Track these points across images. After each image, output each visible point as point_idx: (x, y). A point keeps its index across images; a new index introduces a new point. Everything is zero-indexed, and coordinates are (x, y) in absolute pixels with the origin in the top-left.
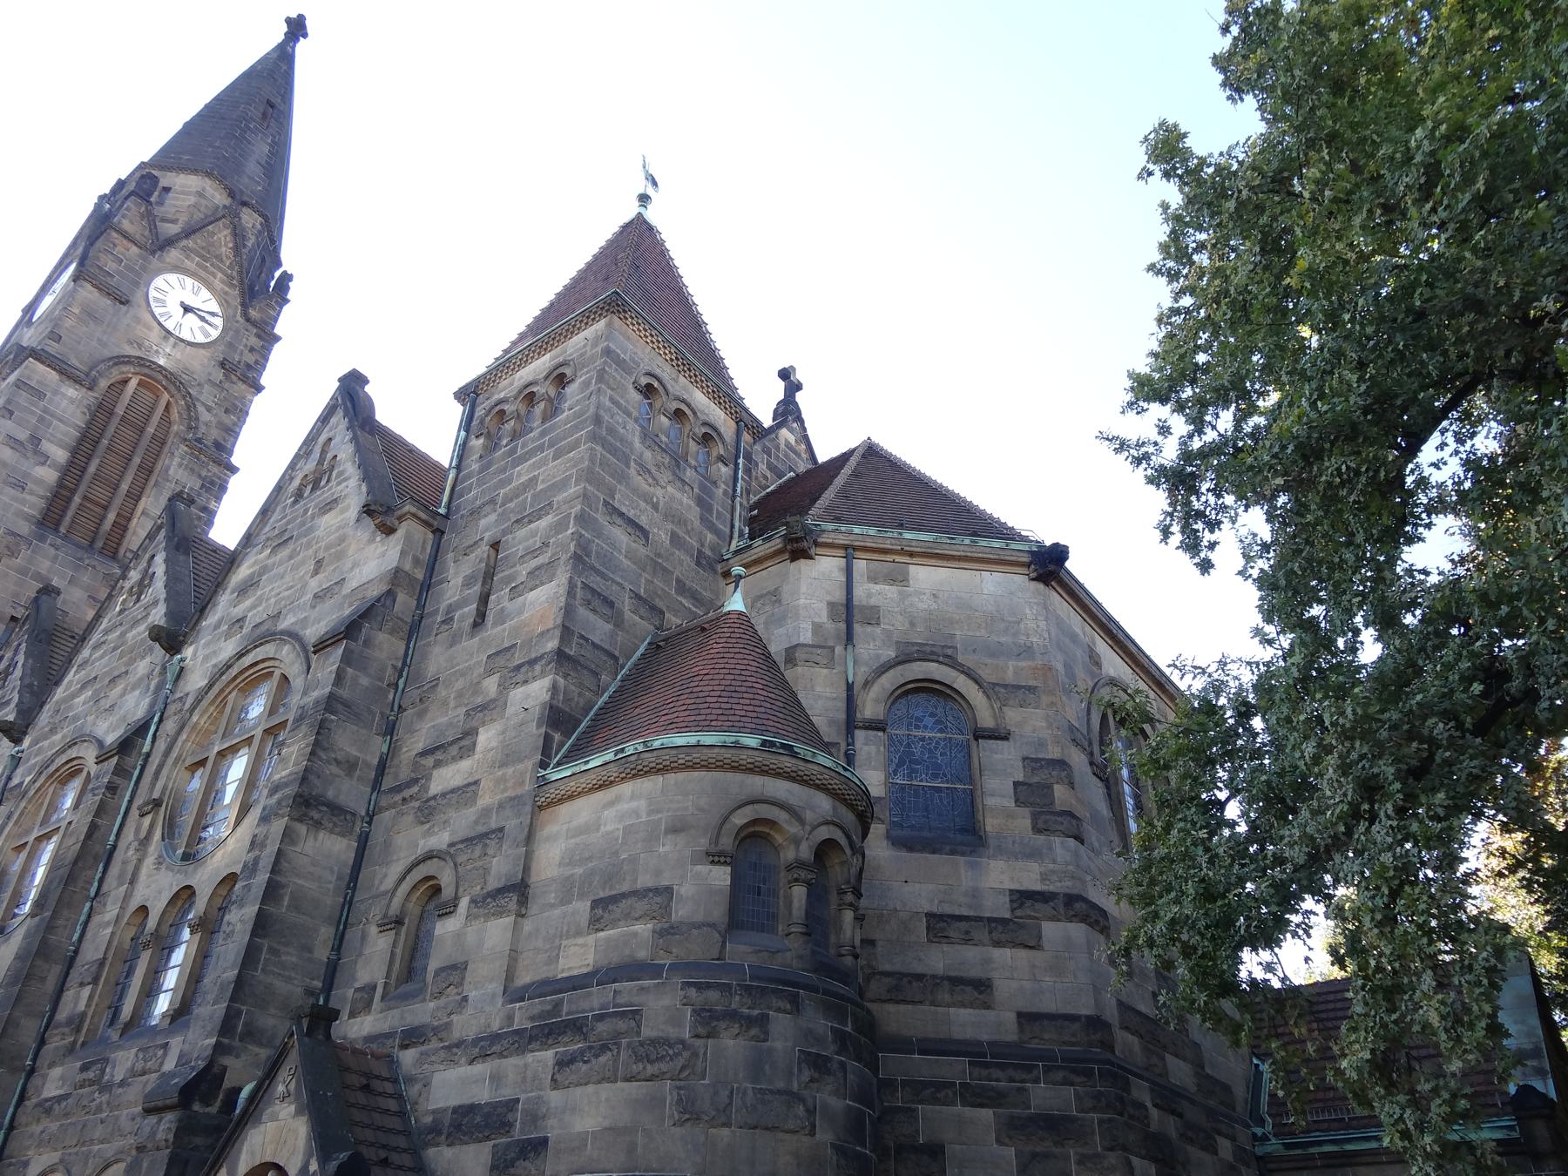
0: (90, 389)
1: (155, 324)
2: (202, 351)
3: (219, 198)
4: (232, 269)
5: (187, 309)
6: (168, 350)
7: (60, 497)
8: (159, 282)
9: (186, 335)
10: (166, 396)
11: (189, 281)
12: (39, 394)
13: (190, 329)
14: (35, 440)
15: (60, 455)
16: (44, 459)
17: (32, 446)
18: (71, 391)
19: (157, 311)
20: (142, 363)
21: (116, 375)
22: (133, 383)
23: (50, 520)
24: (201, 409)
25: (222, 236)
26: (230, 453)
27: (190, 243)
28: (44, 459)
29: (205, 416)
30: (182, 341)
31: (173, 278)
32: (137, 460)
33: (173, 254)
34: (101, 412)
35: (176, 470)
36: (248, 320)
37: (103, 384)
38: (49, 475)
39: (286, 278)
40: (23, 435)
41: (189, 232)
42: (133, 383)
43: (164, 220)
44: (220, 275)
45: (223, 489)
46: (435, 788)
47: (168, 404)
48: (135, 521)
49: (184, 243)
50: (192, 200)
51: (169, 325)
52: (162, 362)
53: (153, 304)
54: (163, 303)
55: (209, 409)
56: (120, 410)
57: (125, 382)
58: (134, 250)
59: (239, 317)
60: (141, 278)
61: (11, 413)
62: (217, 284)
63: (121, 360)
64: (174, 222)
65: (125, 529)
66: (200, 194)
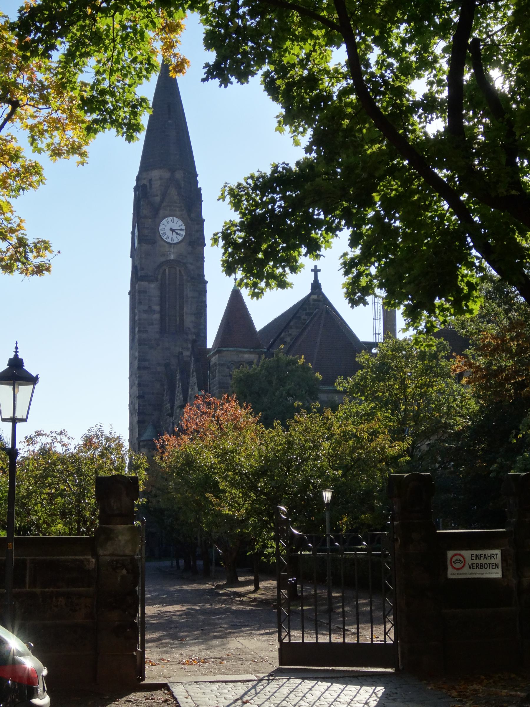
0: (157, 281)
1: (166, 244)
2: (183, 244)
3: (167, 175)
4: (179, 203)
5: (173, 230)
6: (172, 251)
7: (162, 319)
8: (161, 226)
9: (176, 241)
10: (178, 268)
11: (169, 219)
12: (145, 292)
13: (176, 239)
14: (150, 307)
15: (157, 308)
16: (154, 312)
17: (150, 311)
18: (153, 286)
19: (164, 238)
20: (168, 262)
21: (161, 271)
22: (167, 270)
23: (163, 331)
24: (189, 266)
25: (173, 192)
26: (204, 276)
27: (165, 204)
28: (154, 312)
29: (191, 267)
30: (175, 244)
31: (164, 222)
32: (178, 296)
33: (161, 212)
34: (162, 288)
35: (189, 292)
36: (191, 219)
37: (159, 277)
38: (157, 316)
39: (200, 188)
40: (146, 308)
41: (162, 201)
42: (167, 270)
43: (154, 196)
44: (177, 209)
45: (205, 291)
46: (207, 495)
47: (180, 270)
48: (185, 317)
49: (162, 206)
50: (159, 182)
51: (170, 241)
52: (172, 257)
53: (162, 236)
54: (165, 234)
55: (191, 264)
56: (167, 282)
57: (165, 270)
58: (150, 220)
59: (189, 222)
60: (155, 229)
61: (141, 302)
62: (178, 213)
63: (162, 264)
64: (157, 195)
65: (183, 320)
66: (161, 179)
